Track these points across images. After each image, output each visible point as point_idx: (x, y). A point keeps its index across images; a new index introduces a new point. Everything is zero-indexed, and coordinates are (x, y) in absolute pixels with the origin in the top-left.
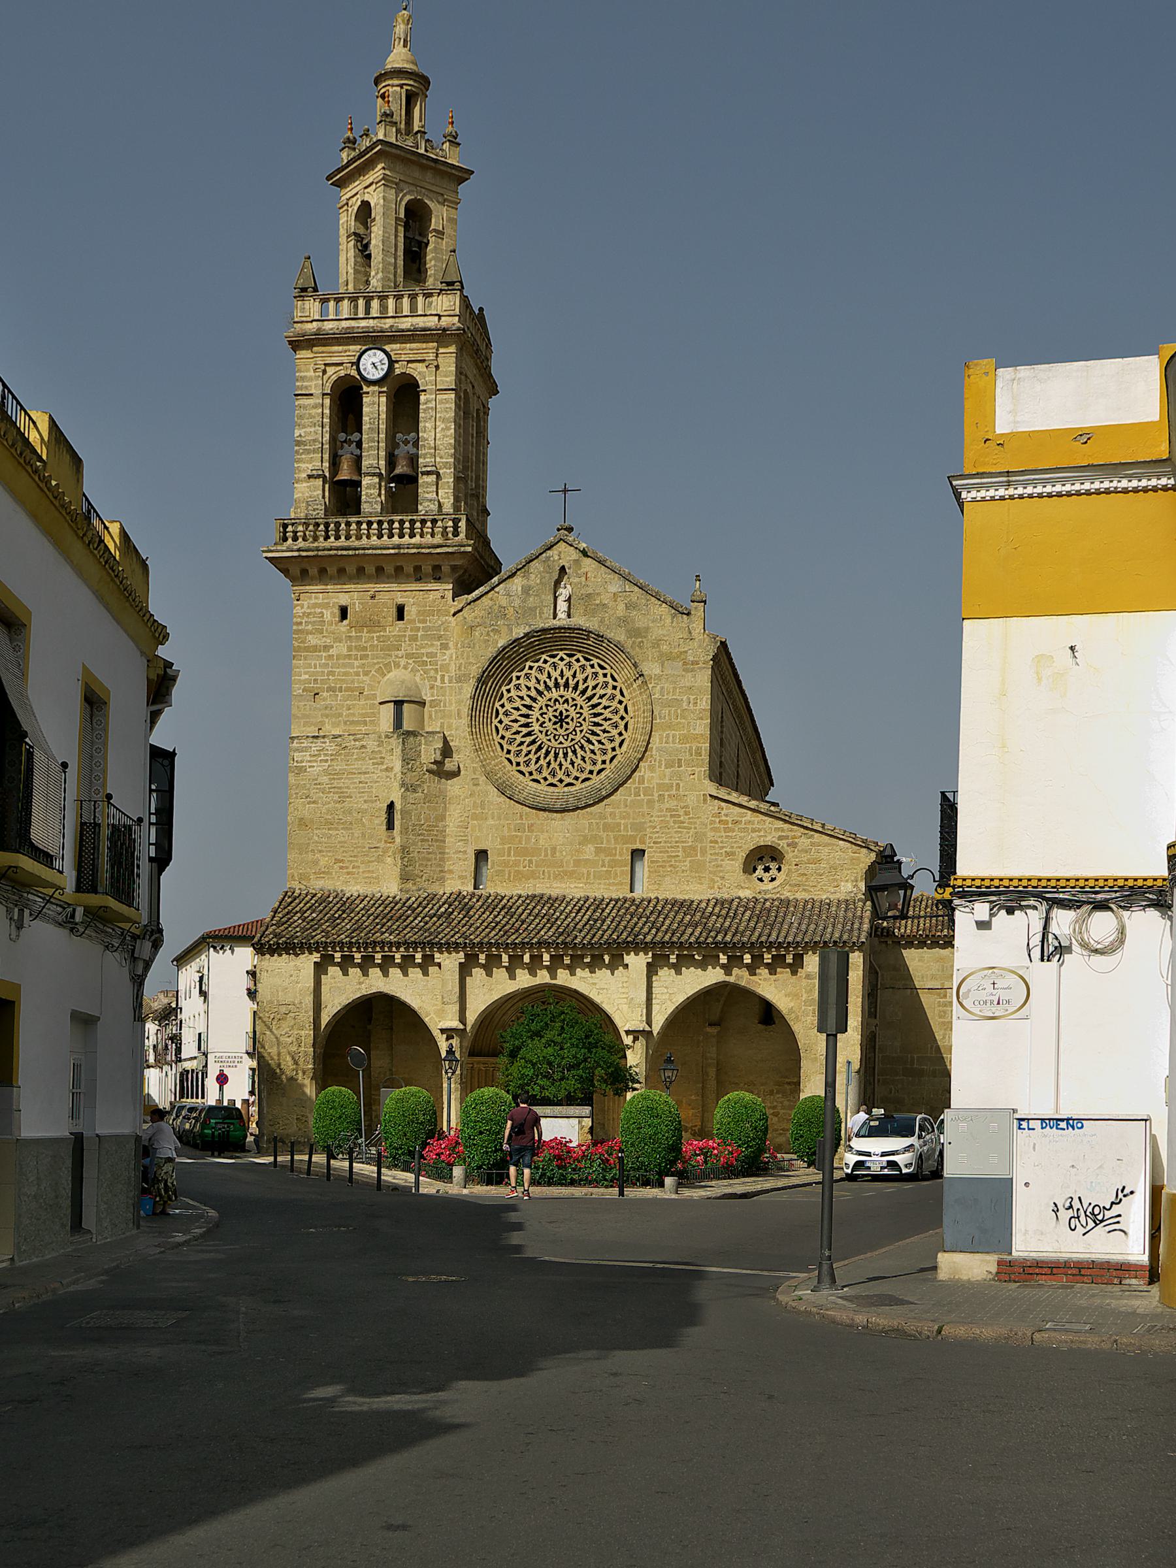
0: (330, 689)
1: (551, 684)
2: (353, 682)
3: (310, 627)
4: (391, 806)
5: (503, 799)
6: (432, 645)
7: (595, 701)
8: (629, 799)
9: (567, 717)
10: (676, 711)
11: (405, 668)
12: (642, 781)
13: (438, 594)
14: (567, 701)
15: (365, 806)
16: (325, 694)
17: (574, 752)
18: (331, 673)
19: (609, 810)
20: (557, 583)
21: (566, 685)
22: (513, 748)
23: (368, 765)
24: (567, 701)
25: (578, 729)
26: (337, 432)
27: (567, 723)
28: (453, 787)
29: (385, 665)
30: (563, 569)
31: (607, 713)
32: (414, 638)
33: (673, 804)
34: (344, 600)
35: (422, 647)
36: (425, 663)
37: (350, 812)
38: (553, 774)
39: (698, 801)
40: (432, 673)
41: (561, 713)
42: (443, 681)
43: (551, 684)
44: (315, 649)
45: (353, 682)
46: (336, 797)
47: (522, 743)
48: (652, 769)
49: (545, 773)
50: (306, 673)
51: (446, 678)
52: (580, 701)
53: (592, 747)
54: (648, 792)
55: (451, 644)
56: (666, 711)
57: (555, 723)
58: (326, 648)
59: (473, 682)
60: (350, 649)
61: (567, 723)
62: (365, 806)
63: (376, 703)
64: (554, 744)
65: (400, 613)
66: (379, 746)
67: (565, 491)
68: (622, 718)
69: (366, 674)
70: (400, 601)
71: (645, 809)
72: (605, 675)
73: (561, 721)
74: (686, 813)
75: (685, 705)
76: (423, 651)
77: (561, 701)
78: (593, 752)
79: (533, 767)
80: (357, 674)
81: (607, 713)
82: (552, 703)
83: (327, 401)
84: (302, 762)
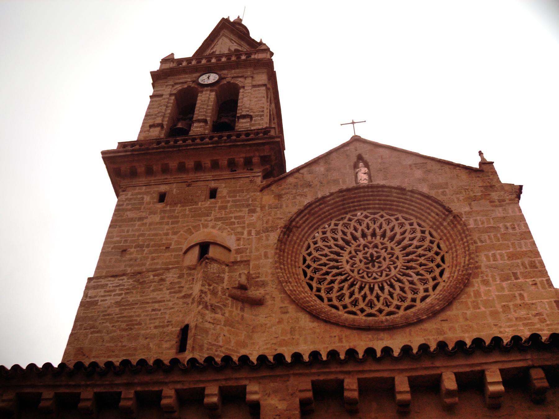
0: (137, 246)
1: (358, 234)
2: (161, 240)
3: (130, 207)
4: (185, 330)
5: (315, 324)
6: (241, 211)
7: (406, 242)
8: (468, 312)
9: (378, 257)
10: (495, 236)
11: (213, 227)
12: (477, 294)
13: (248, 180)
14: (376, 246)
15: (155, 331)
16: (132, 250)
17: (392, 286)
18: (143, 235)
19: (446, 326)
20: (356, 166)
21: (374, 235)
22: (323, 286)
23: (165, 294)
24: (376, 246)
25: (392, 267)
26: (179, 120)
27: (380, 263)
28: (261, 316)
29: (194, 227)
30: (360, 158)
31: (420, 251)
32: (224, 208)
33: (523, 313)
34: (163, 188)
35: (231, 212)
36: (234, 223)
37: (136, 338)
38: (371, 304)
39: (551, 308)
40: (239, 230)
41: (372, 255)
42: (249, 233)
43: (358, 234)
44: (132, 220)
45: (161, 240)
46: (124, 325)
47: (332, 282)
48: (486, 283)
49: (362, 305)
50: (117, 236)
51: (253, 233)
52: (389, 245)
53: (410, 279)
54: (486, 303)
55: (258, 209)
56: (485, 236)
57: (366, 264)
58: (141, 219)
59: (279, 231)
60: (162, 218)
61: (380, 263)
62: (155, 331)
63: (181, 253)
64: (367, 279)
65: (213, 194)
66: (179, 277)
67: (353, 123)
68: (437, 254)
69: (175, 233)
70: (213, 185)
71: (490, 320)
72: (411, 224)
73: (372, 261)
74: (543, 321)
75: (503, 230)
76: (233, 215)
77: (370, 246)
78: (412, 283)
79: (347, 300)
80: (167, 234)
81: (420, 251)
82: (361, 248)
83: (173, 98)
84: (95, 297)
